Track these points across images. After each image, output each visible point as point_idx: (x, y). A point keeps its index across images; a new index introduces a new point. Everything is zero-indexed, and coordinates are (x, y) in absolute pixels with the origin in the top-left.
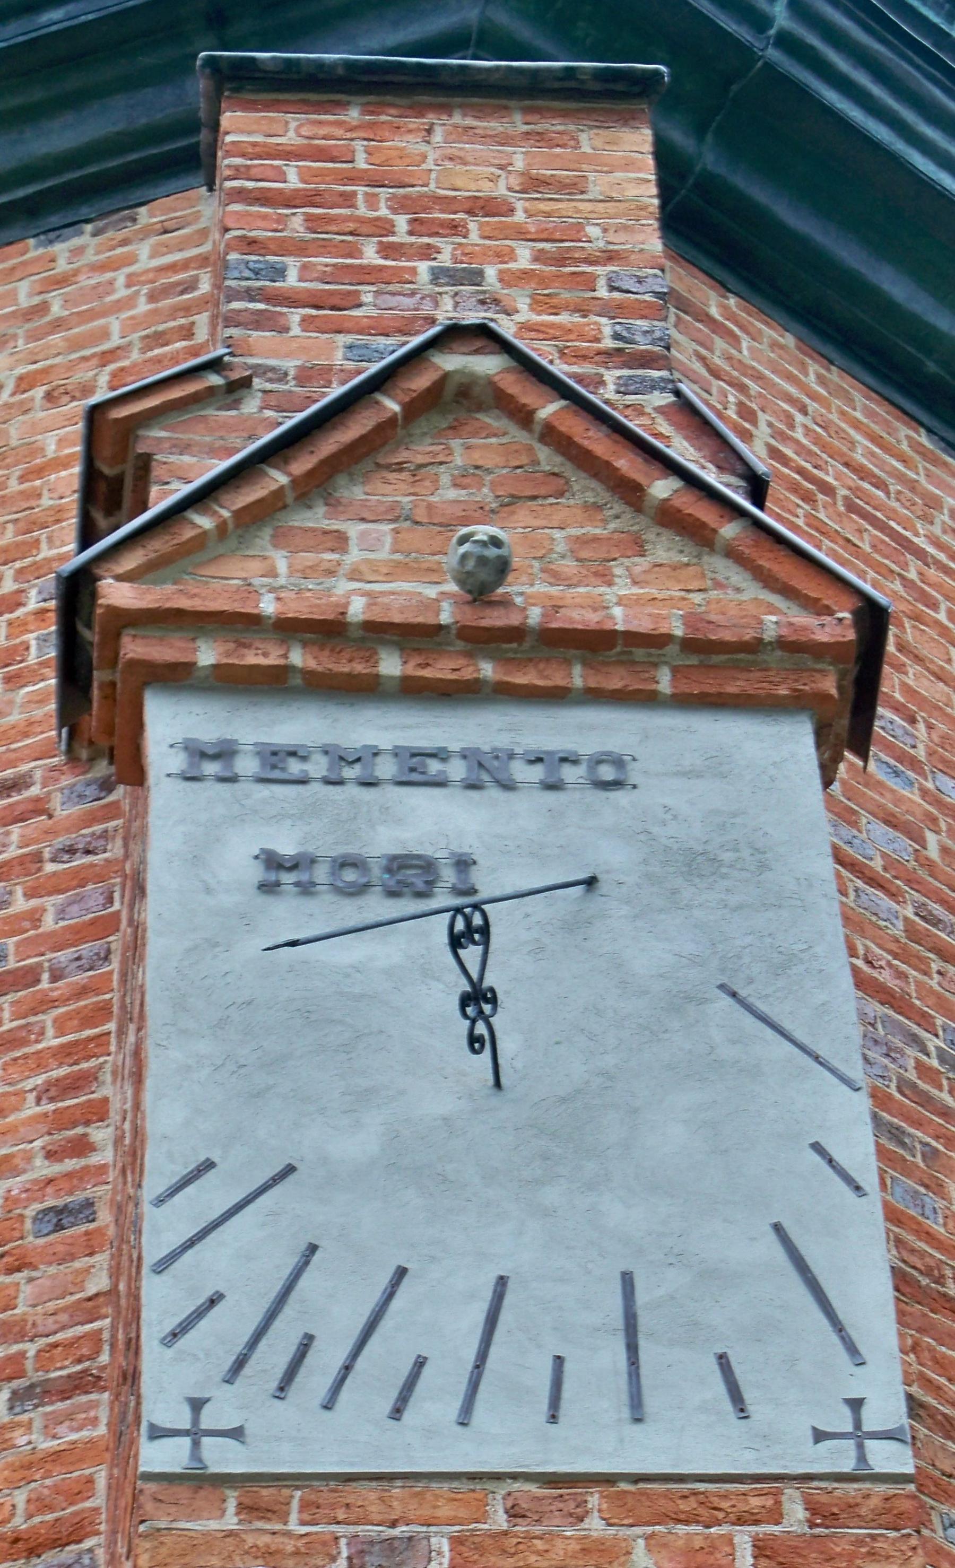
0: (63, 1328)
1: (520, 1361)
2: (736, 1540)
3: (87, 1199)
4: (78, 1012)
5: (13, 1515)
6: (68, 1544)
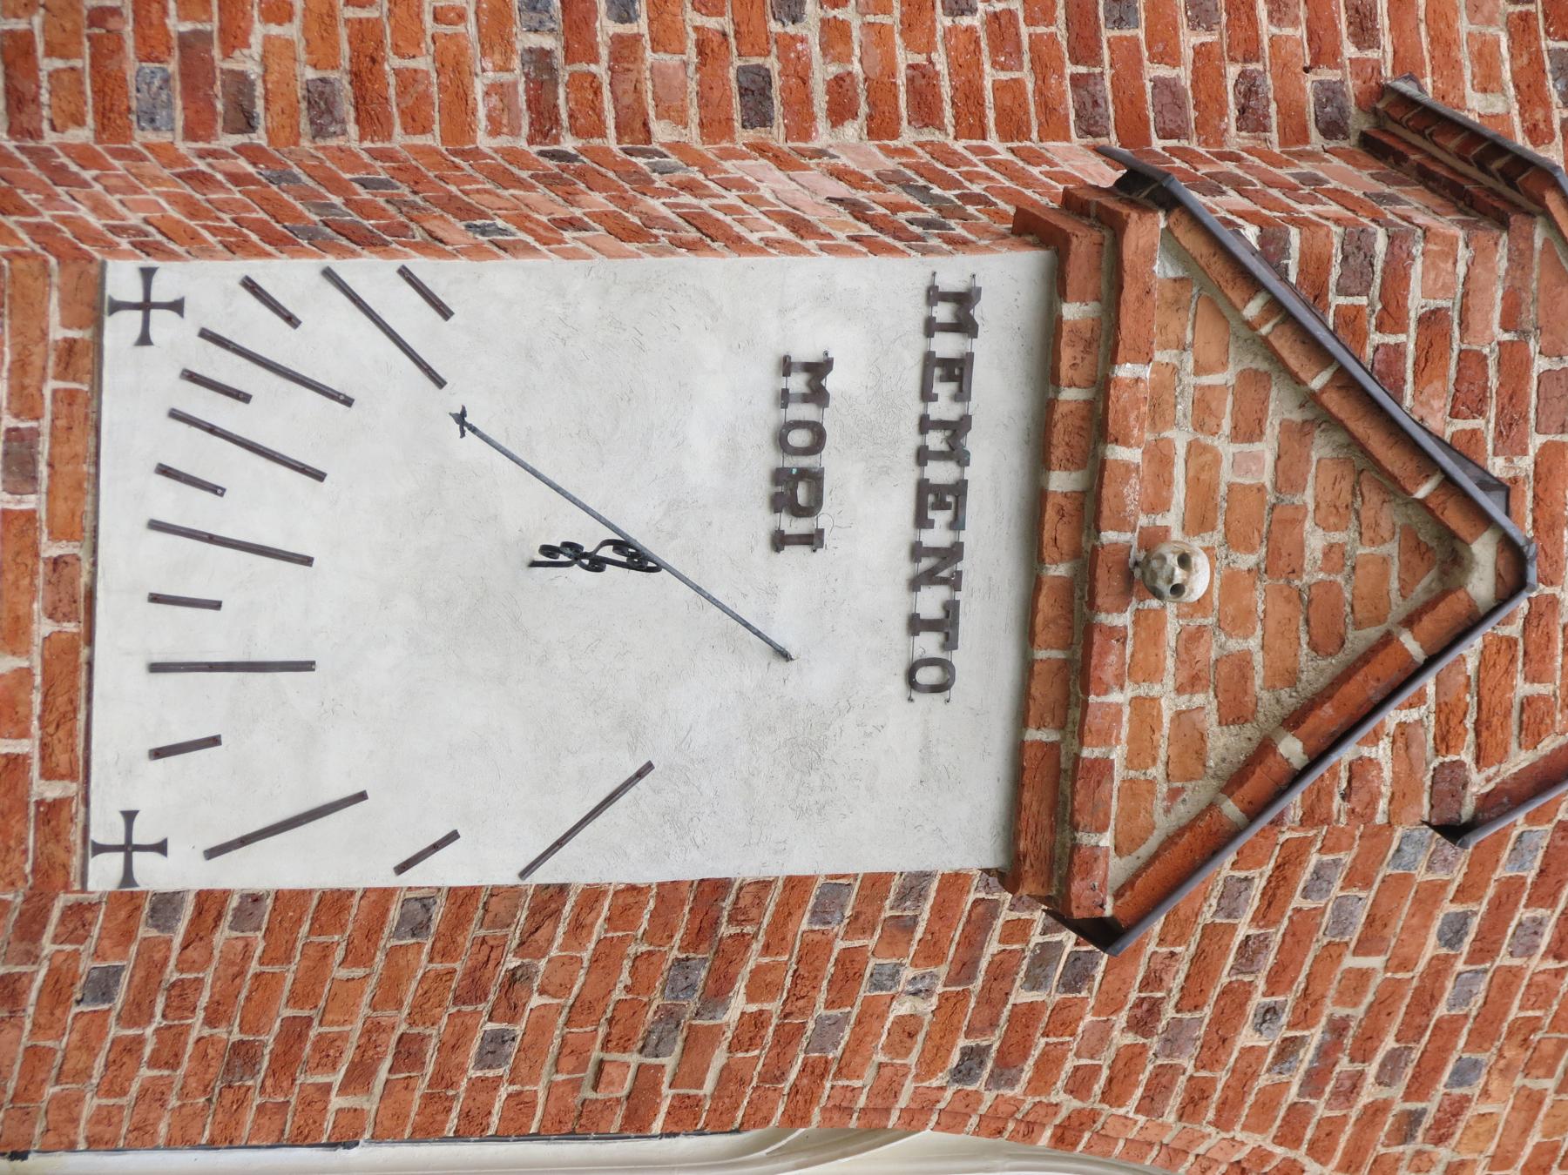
0: (616, 99)
1: (209, 571)
2: (25, 741)
3: (771, 119)
4: (1023, 105)
5: (403, 57)
6: (357, 109)
